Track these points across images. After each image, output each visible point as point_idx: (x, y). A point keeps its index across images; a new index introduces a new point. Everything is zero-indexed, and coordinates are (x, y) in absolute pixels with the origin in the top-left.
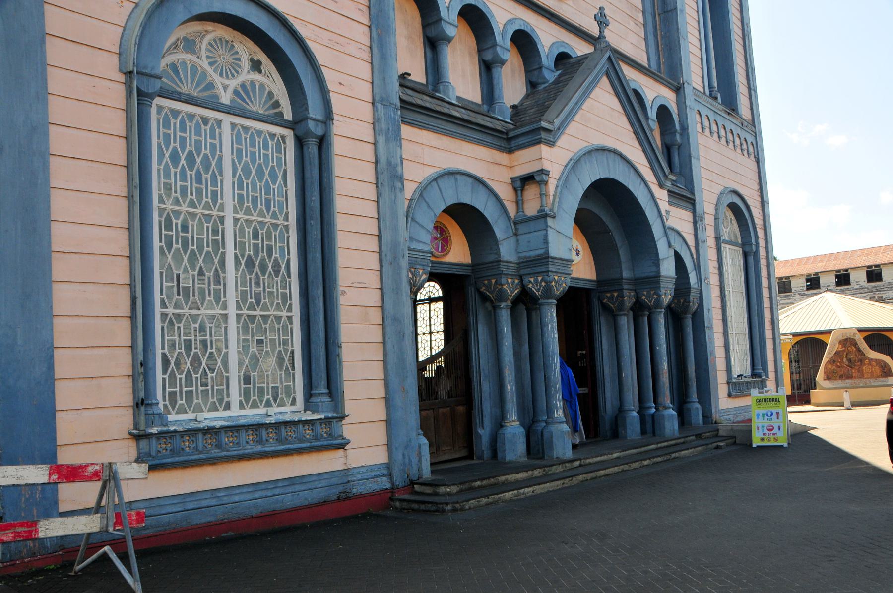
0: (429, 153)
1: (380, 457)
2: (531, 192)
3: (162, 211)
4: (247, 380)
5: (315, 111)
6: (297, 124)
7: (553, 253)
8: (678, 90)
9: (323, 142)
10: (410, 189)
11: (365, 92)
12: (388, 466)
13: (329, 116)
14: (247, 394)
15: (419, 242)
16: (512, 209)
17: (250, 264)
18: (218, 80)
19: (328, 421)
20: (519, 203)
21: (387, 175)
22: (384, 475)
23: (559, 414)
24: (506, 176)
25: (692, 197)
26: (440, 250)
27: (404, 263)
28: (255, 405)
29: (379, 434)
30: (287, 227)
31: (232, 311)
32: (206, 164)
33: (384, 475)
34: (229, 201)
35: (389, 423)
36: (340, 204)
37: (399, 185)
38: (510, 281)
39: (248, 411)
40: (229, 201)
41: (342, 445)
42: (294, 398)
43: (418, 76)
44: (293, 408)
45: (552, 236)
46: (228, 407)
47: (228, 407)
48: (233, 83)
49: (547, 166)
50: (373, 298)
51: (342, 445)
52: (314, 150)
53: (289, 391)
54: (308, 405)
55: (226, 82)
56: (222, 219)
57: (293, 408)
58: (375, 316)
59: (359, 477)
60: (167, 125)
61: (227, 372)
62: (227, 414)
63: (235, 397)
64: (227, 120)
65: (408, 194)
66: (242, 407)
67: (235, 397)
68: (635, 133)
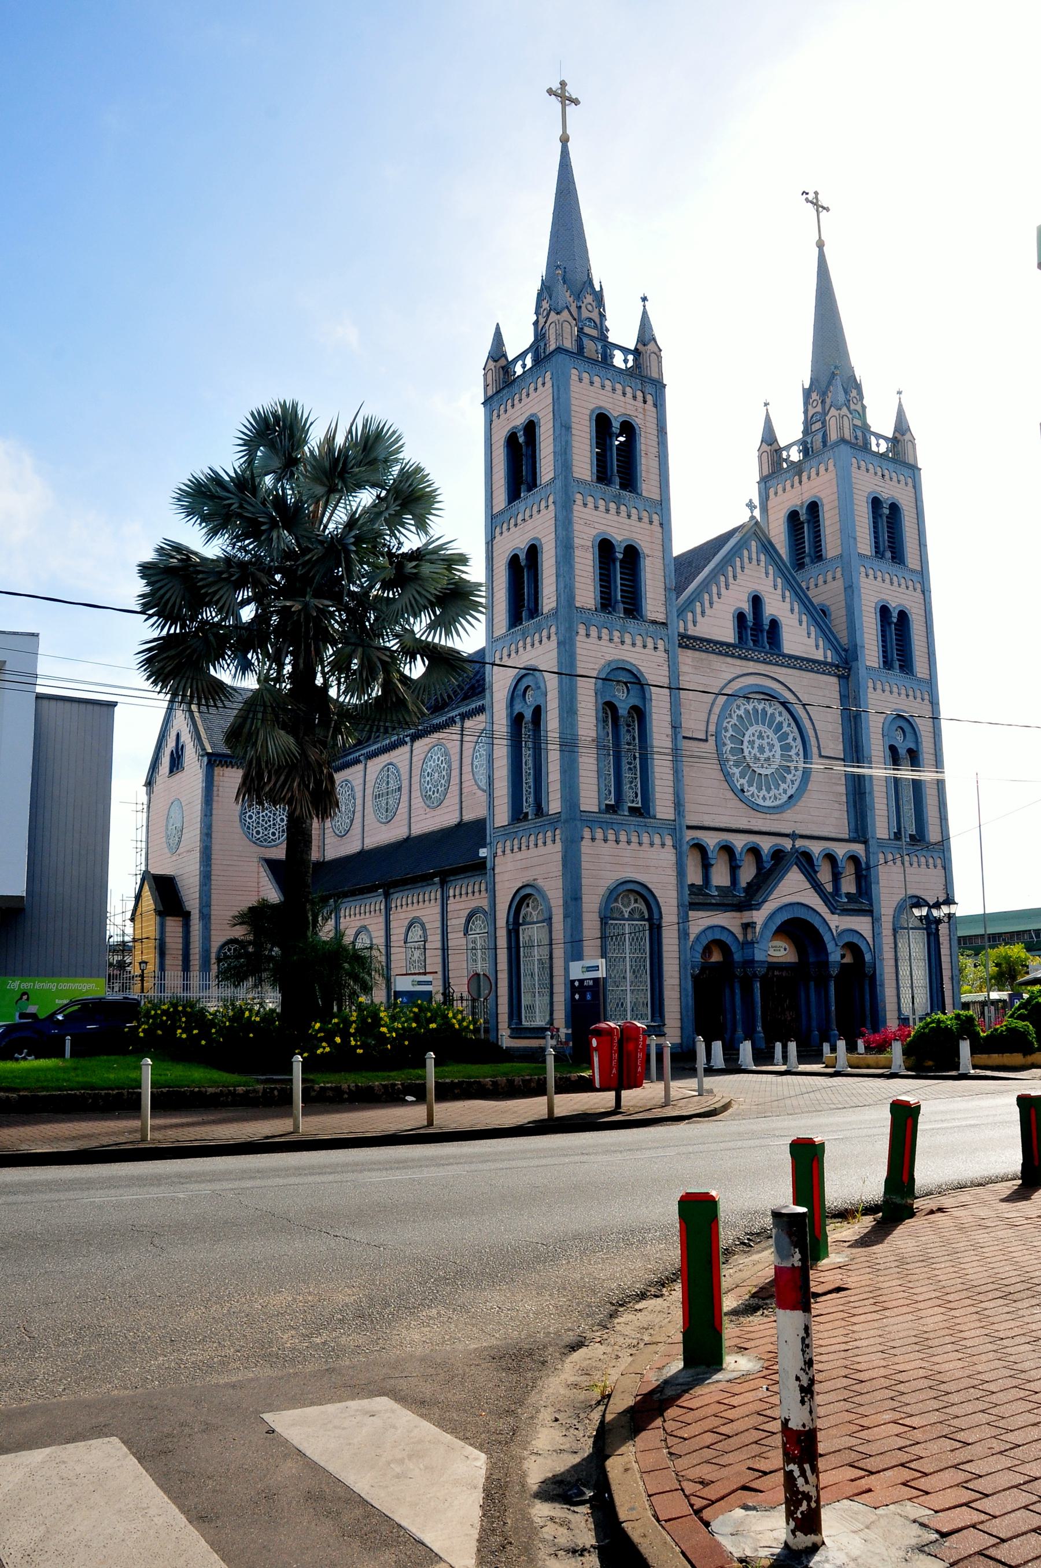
0: (701, 921)
2: (749, 930)
5: (656, 916)
6: (650, 920)
7: (756, 959)
8: (865, 842)
9: (659, 927)
10: (692, 937)
11: (674, 902)
12: (681, 1044)
13: (661, 917)
16: (741, 938)
17: (634, 972)
18: (624, 910)
19: (659, 1026)
20: (745, 935)
21: (683, 934)
23: (759, 1029)
24: (738, 922)
27: (689, 967)
29: (678, 1032)
34: (628, 951)
35: (682, 1028)
36: (665, 948)
40: (628, 951)
43: (699, 882)
45: (756, 951)
48: (629, 910)
49: (755, 920)
50: (677, 982)
52: (656, 930)
53: (646, 1015)
54: (652, 1021)
64: (627, 923)
65: (691, 939)
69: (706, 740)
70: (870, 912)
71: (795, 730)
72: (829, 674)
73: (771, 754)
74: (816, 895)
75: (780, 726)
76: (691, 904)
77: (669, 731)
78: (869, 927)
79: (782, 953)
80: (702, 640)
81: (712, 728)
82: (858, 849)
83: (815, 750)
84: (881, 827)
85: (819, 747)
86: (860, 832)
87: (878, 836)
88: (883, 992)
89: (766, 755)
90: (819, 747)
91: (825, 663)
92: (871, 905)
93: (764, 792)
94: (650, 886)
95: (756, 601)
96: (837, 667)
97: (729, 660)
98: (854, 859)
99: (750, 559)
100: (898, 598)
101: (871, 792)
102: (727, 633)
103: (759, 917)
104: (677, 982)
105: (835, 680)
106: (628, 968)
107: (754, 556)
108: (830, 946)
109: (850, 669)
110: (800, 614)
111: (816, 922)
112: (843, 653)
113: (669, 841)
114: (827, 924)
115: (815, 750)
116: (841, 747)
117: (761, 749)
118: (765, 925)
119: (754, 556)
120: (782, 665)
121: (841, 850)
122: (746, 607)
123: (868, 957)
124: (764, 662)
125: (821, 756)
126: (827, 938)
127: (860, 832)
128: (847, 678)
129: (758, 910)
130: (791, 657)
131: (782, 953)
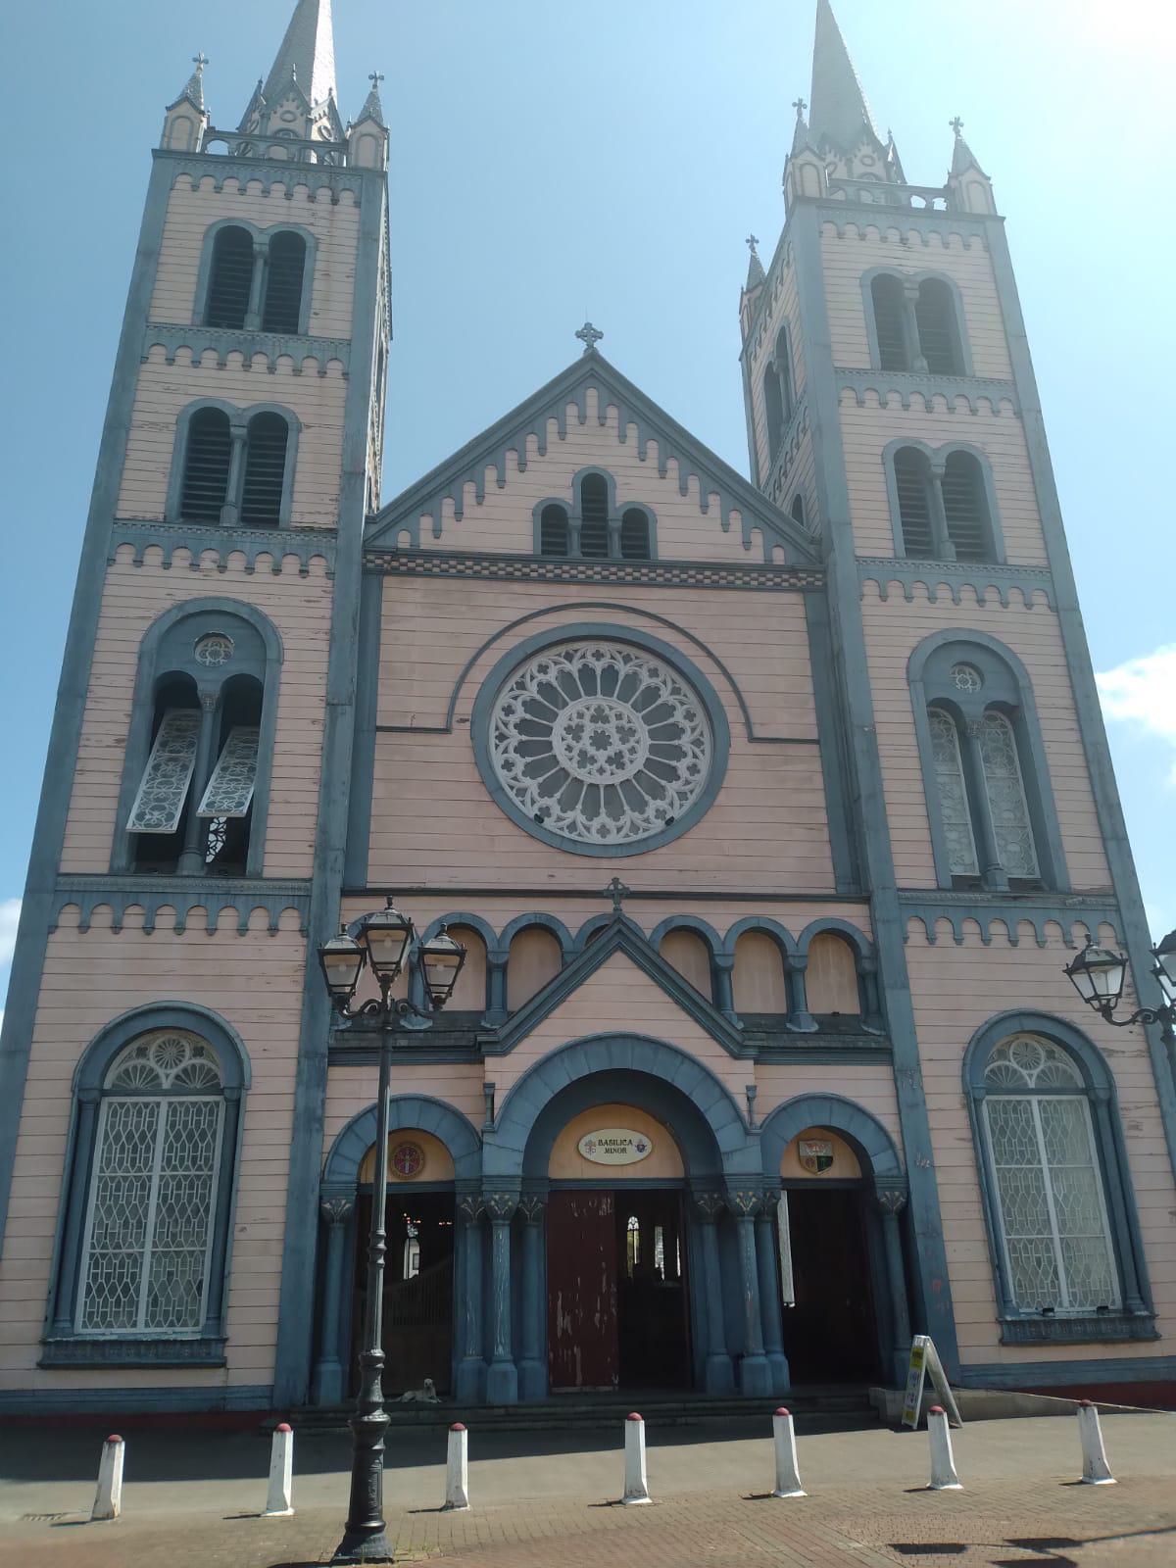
1: (263, 1378)
3: (100, 1179)
4: (155, 1302)
8: (867, 900)
10: (334, 1127)
12: (271, 1388)
14: (153, 1316)
15: (341, 1173)
18: (161, 1072)
21: (308, 1119)
22: (266, 1397)
25: (887, 1045)
26: (407, 1169)
28: (159, 1325)
29: (267, 1358)
30: (210, 1177)
31: (148, 1248)
32: (143, 1137)
33: (266, 1397)
34: (158, 1163)
37: (317, 1126)
38: (470, 1200)
39: (152, 1329)
40: (158, 1163)
41: (222, 1364)
42: (198, 1320)
44: (195, 1329)
46: (134, 1325)
47: (134, 1325)
48: (174, 1072)
51: (222, 1364)
53: (194, 1314)
55: (169, 1072)
56: (150, 1178)
57: (195, 1329)
58: (277, 1249)
59: (238, 1395)
60: (115, 1114)
61: (138, 1296)
62: (133, 1330)
63: (142, 1317)
64: (164, 1101)
66: (147, 1325)
67: (142, 1317)
68: (677, 1002)
69: (446, 731)
70: (882, 1053)
71: (692, 697)
72: (777, 588)
73: (625, 748)
74: (683, 1016)
75: (652, 693)
76: (332, 1051)
77: (320, 713)
78: (886, 1088)
79: (632, 1155)
80: (461, 556)
81: (464, 708)
82: (852, 915)
83: (737, 730)
84: (910, 862)
85: (748, 724)
86: (856, 879)
87: (901, 884)
88: (938, 1254)
89: (611, 751)
90: (748, 724)
91: (766, 568)
92: (888, 1038)
93: (603, 818)
94: (223, 1017)
95: (594, 487)
96: (793, 571)
97: (517, 587)
98: (836, 934)
99: (582, 419)
100: (938, 425)
101: (877, 794)
102: (519, 537)
103: (504, 1071)
104: (276, 1232)
105: (794, 598)
106: (153, 1201)
107: (592, 411)
108: (727, 1137)
109: (824, 572)
110: (704, 493)
111: (682, 1079)
112: (812, 550)
113: (290, 921)
114: (717, 1082)
115: (737, 730)
116: (812, 718)
117: (601, 741)
118: (520, 1089)
119: (592, 411)
120: (651, 584)
121: (795, 922)
122: (567, 495)
123: (881, 1164)
124: (605, 582)
125: (753, 739)
126: (715, 1116)
127: (856, 879)
128: (824, 590)
129: (504, 1053)
130: (669, 566)
131: (632, 1155)
